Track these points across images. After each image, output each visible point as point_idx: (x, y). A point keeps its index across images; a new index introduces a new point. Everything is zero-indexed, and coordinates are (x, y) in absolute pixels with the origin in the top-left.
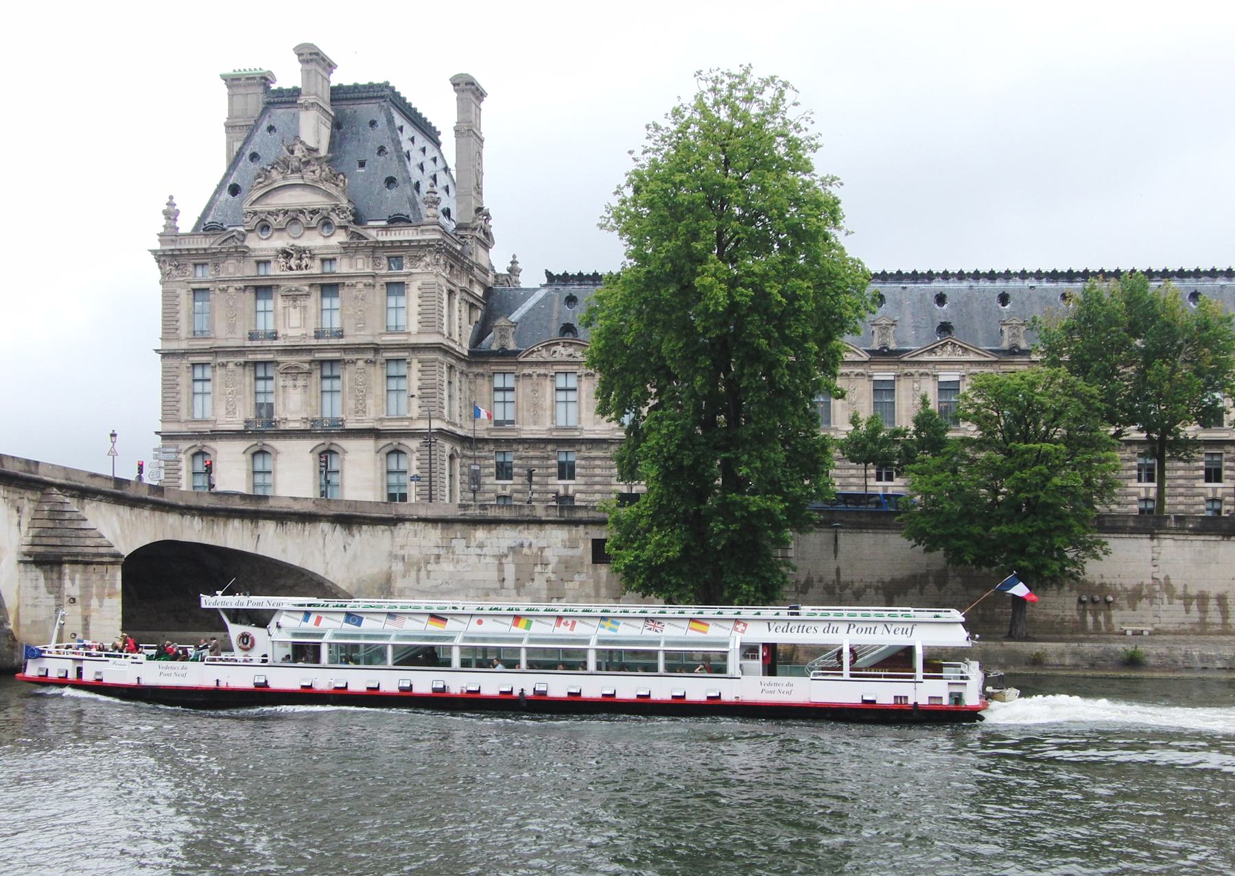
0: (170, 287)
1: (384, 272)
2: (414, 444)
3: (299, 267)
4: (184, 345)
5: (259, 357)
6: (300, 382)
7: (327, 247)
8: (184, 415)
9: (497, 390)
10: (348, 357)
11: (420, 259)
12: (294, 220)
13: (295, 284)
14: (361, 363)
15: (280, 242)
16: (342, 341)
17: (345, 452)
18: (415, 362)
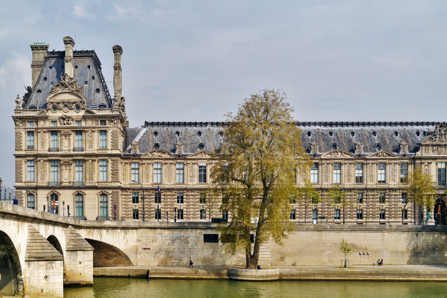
0: (18, 130)
1: (100, 126)
2: (110, 191)
3: (68, 124)
4: (23, 153)
5: (53, 158)
6: (68, 168)
7: (78, 116)
8: (24, 180)
9: (132, 169)
10: (86, 159)
11: (112, 122)
12: (66, 106)
13: (66, 130)
14: (90, 161)
15: (59, 114)
16: (84, 153)
17: (85, 194)
18: (110, 161)
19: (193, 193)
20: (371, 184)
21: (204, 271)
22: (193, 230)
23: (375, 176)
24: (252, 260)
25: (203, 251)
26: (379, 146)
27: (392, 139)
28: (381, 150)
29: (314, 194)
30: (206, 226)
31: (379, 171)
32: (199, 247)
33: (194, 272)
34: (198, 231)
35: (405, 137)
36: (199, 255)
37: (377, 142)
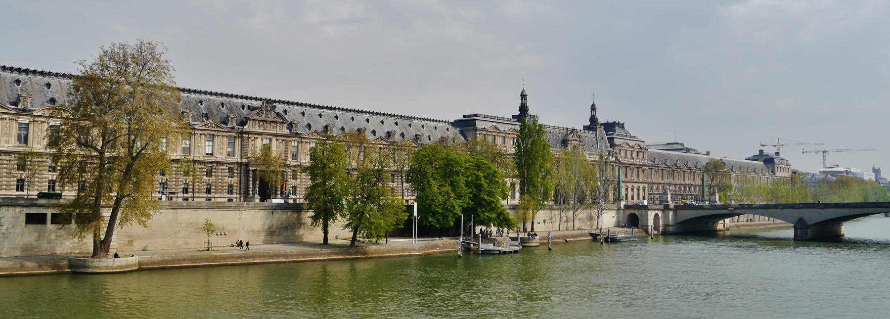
19: (8, 158)
20: (199, 156)
21: (34, 264)
22: (11, 208)
23: (204, 148)
24: (102, 247)
25: (28, 235)
26: (207, 116)
27: (218, 110)
28: (210, 121)
29: (189, 166)
30: (30, 203)
31: (207, 143)
32: (17, 231)
33: (18, 266)
34: (18, 209)
35: (231, 109)
36: (16, 242)
37: (204, 112)
